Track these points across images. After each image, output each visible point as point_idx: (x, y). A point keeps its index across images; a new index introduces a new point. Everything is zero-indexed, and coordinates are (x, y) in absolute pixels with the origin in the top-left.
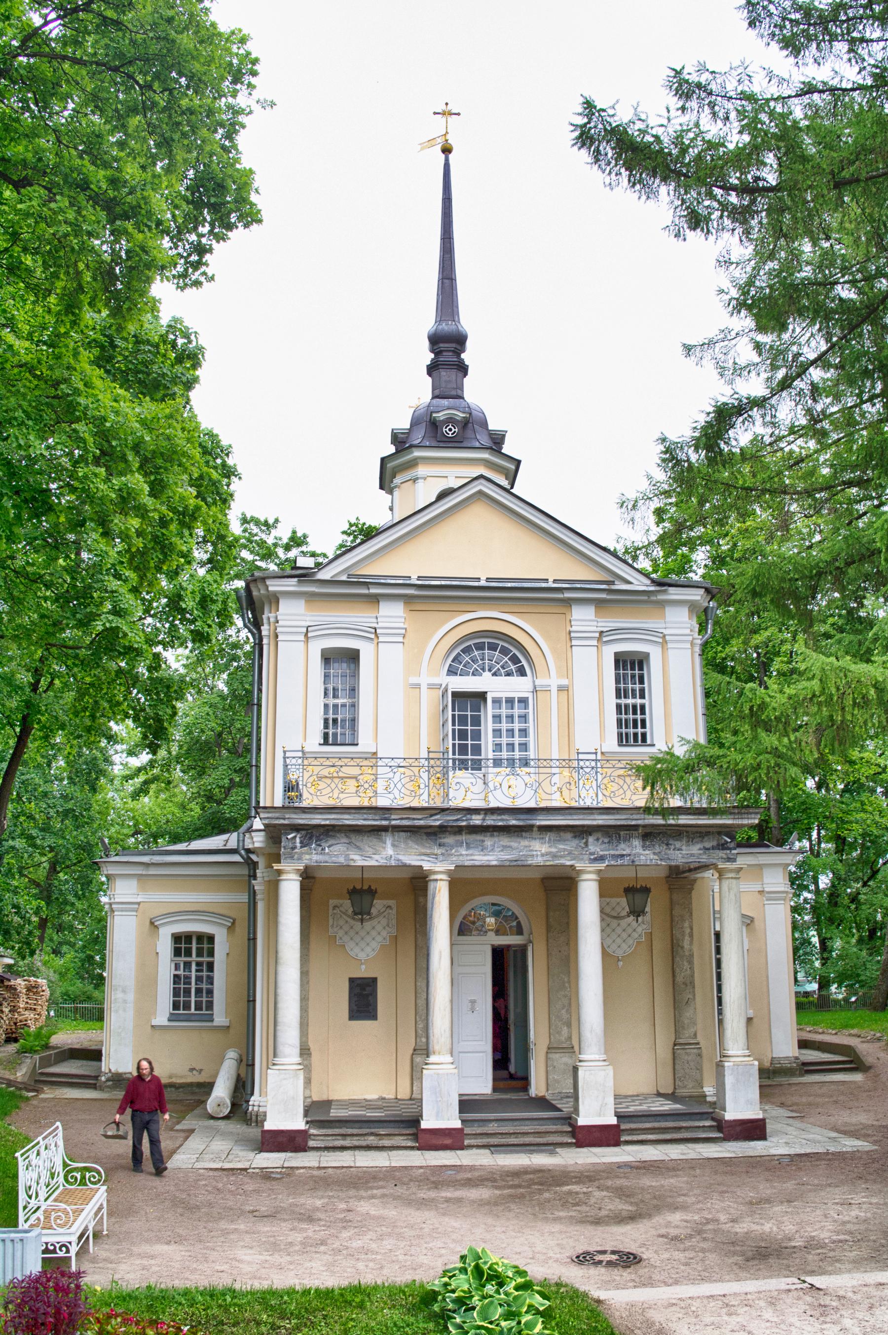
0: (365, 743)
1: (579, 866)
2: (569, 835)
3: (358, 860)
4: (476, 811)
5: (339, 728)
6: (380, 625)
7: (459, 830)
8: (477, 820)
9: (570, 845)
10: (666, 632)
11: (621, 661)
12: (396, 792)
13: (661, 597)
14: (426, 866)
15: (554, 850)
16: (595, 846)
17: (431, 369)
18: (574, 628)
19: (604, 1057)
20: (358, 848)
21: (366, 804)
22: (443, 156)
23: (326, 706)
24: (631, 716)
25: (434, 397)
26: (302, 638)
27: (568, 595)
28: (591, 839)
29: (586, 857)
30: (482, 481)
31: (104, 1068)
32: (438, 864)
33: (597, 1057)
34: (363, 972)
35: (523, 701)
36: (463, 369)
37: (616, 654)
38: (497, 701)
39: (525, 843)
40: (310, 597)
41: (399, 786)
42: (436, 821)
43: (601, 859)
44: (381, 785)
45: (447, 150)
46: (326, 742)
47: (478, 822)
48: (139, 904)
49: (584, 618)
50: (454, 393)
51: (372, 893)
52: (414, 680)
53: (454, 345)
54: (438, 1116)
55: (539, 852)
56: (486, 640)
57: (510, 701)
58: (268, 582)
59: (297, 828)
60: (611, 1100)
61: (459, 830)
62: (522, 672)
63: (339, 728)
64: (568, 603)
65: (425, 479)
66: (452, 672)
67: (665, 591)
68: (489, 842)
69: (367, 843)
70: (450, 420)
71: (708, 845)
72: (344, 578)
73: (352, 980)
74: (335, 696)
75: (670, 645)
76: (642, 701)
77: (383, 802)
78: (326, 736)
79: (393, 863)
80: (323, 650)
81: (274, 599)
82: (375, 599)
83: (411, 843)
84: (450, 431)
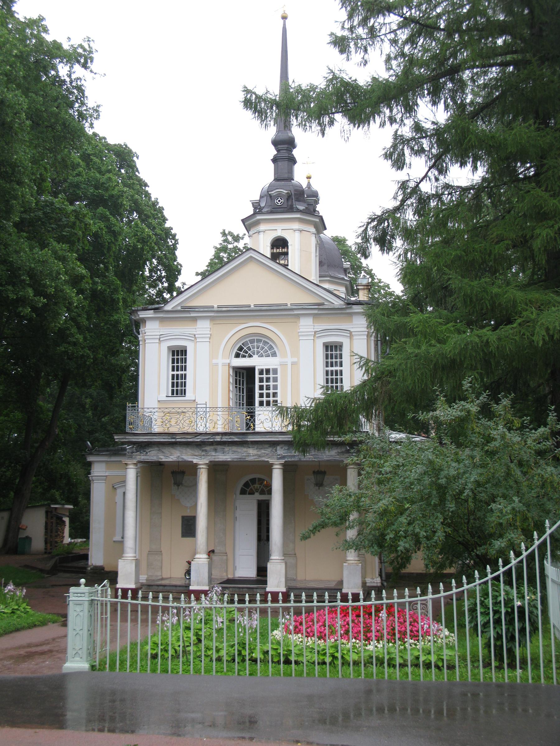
0: (189, 395)
1: (271, 461)
2: (267, 446)
3: (163, 459)
4: (218, 434)
5: (178, 387)
6: (198, 332)
7: (212, 444)
8: (218, 439)
9: (268, 451)
10: (352, 330)
11: (328, 347)
12: (181, 425)
13: (348, 311)
14: (195, 461)
15: (259, 453)
16: (281, 451)
17: (275, 160)
18: (301, 330)
19: (283, 558)
20: (163, 452)
21: (166, 431)
22: (282, 21)
23: (173, 376)
24: (334, 377)
25: (276, 179)
26: (157, 341)
27: (296, 312)
28: (278, 448)
29: (275, 457)
30: (251, 251)
31: (90, 563)
32: (201, 460)
33: (277, 558)
34: (188, 513)
35: (275, 371)
36: (293, 161)
37: (324, 344)
38: (261, 372)
39: (245, 449)
40: (162, 320)
41: (182, 422)
42: (198, 439)
43: (283, 457)
44: (173, 422)
45: (284, 18)
46: (173, 393)
47: (219, 440)
48: (106, 476)
49: (307, 325)
50: (286, 176)
51: (183, 473)
52: (214, 361)
53: (286, 146)
54: (198, 584)
55: (251, 454)
56: (256, 338)
57: (268, 371)
58: (139, 313)
59: (134, 443)
60: (283, 580)
61: (212, 444)
62: (274, 355)
63: (178, 387)
64: (298, 316)
65: (264, 232)
66: (237, 355)
67: (351, 308)
68: (227, 449)
69: (167, 450)
70: (279, 195)
71: (343, 450)
72: (179, 308)
73: (183, 518)
74: (177, 370)
75: (355, 337)
76: (341, 368)
77: (173, 430)
78: (173, 391)
79: (180, 460)
80: (169, 348)
81: (144, 320)
82: (195, 319)
83: (188, 450)
84: (279, 202)
